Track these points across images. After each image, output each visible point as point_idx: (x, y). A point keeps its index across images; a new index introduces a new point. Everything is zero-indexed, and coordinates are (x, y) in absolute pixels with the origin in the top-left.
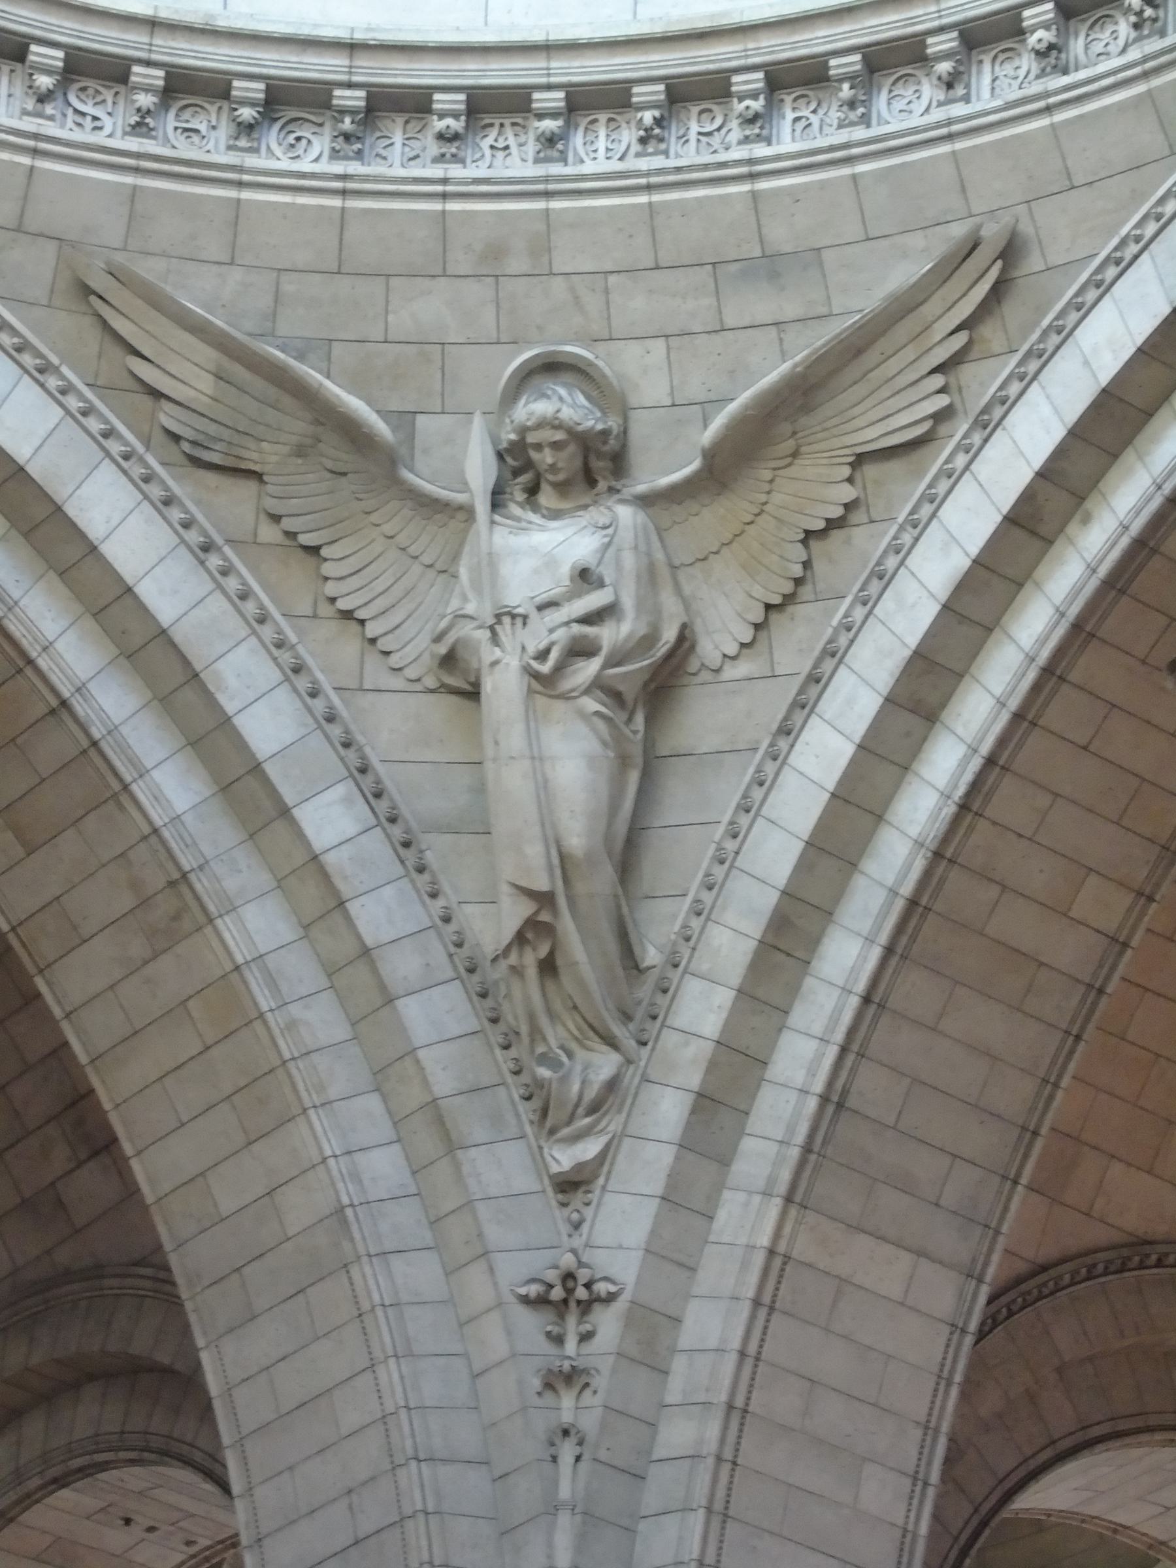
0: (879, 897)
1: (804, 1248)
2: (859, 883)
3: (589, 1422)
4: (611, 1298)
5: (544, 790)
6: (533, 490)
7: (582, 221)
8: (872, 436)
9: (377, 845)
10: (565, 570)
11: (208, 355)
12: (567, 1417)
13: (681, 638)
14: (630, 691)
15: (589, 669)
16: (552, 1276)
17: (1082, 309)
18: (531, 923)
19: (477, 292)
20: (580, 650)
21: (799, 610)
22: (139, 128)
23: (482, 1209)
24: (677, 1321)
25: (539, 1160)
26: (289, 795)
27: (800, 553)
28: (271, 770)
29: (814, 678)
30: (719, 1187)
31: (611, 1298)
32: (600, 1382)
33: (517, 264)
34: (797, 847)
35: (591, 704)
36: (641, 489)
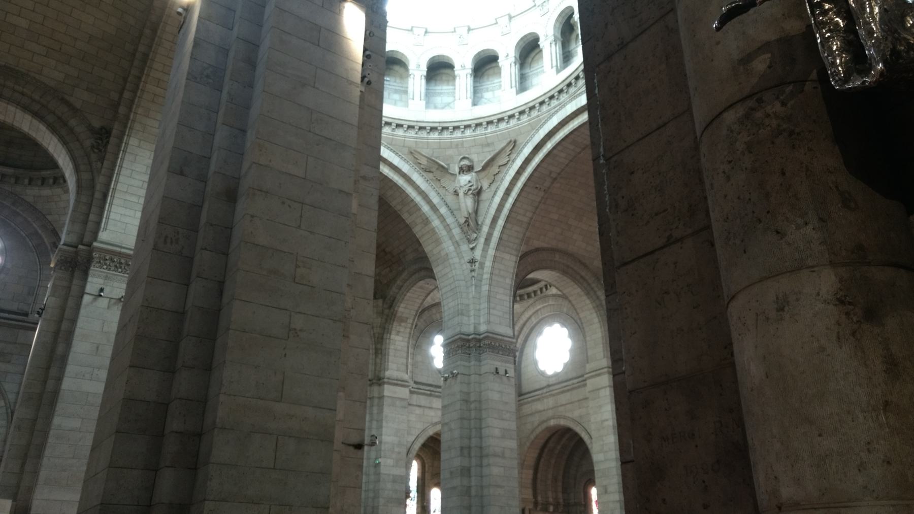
1: (498, 255)
2: (502, 214)
3: (476, 275)
5: (467, 206)
6: (463, 172)
7: (466, 141)
8: (501, 163)
9: (449, 213)
11: (426, 159)
14: (475, 194)
15: (471, 192)
17: (523, 148)
22: (416, 134)
24: (484, 263)
25: (468, 246)
28: (436, 206)
30: (488, 248)
31: (477, 261)
32: (477, 271)
35: (471, 196)
36: (475, 171)
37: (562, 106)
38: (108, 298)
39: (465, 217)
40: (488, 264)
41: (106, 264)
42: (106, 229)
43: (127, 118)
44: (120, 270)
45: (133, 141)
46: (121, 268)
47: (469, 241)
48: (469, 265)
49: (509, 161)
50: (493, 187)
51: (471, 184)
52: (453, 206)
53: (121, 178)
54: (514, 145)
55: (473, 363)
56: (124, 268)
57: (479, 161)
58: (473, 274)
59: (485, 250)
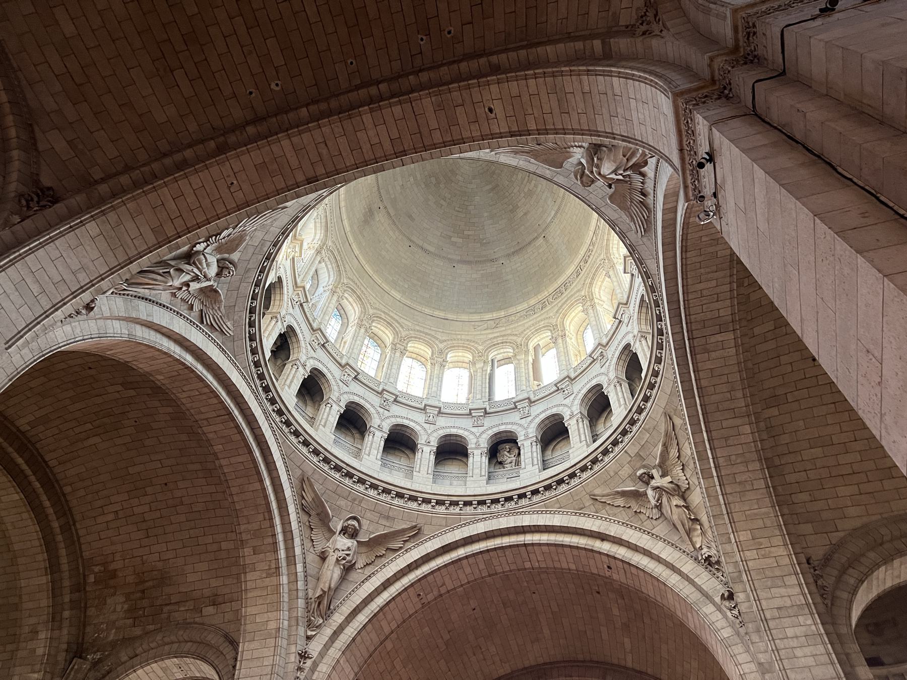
4: (311, 658)
6: (344, 534)
8: (390, 546)
10: (346, 547)
11: (313, 495)
12: (298, 675)
13: (355, 562)
14: (346, 567)
16: (304, 651)
18: (321, 595)
19: (350, 504)
20: (344, 559)
21: (371, 566)
27: (374, 558)
29: (370, 576)
31: (311, 658)
32: (306, 671)
35: (342, 567)
37: (497, 516)
39: (322, 590)
43: (102, 201)
45: (92, 228)
47: (310, 625)
49: (401, 548)
52: (312, 570)
54: (415, 533)
59: (327, 647)
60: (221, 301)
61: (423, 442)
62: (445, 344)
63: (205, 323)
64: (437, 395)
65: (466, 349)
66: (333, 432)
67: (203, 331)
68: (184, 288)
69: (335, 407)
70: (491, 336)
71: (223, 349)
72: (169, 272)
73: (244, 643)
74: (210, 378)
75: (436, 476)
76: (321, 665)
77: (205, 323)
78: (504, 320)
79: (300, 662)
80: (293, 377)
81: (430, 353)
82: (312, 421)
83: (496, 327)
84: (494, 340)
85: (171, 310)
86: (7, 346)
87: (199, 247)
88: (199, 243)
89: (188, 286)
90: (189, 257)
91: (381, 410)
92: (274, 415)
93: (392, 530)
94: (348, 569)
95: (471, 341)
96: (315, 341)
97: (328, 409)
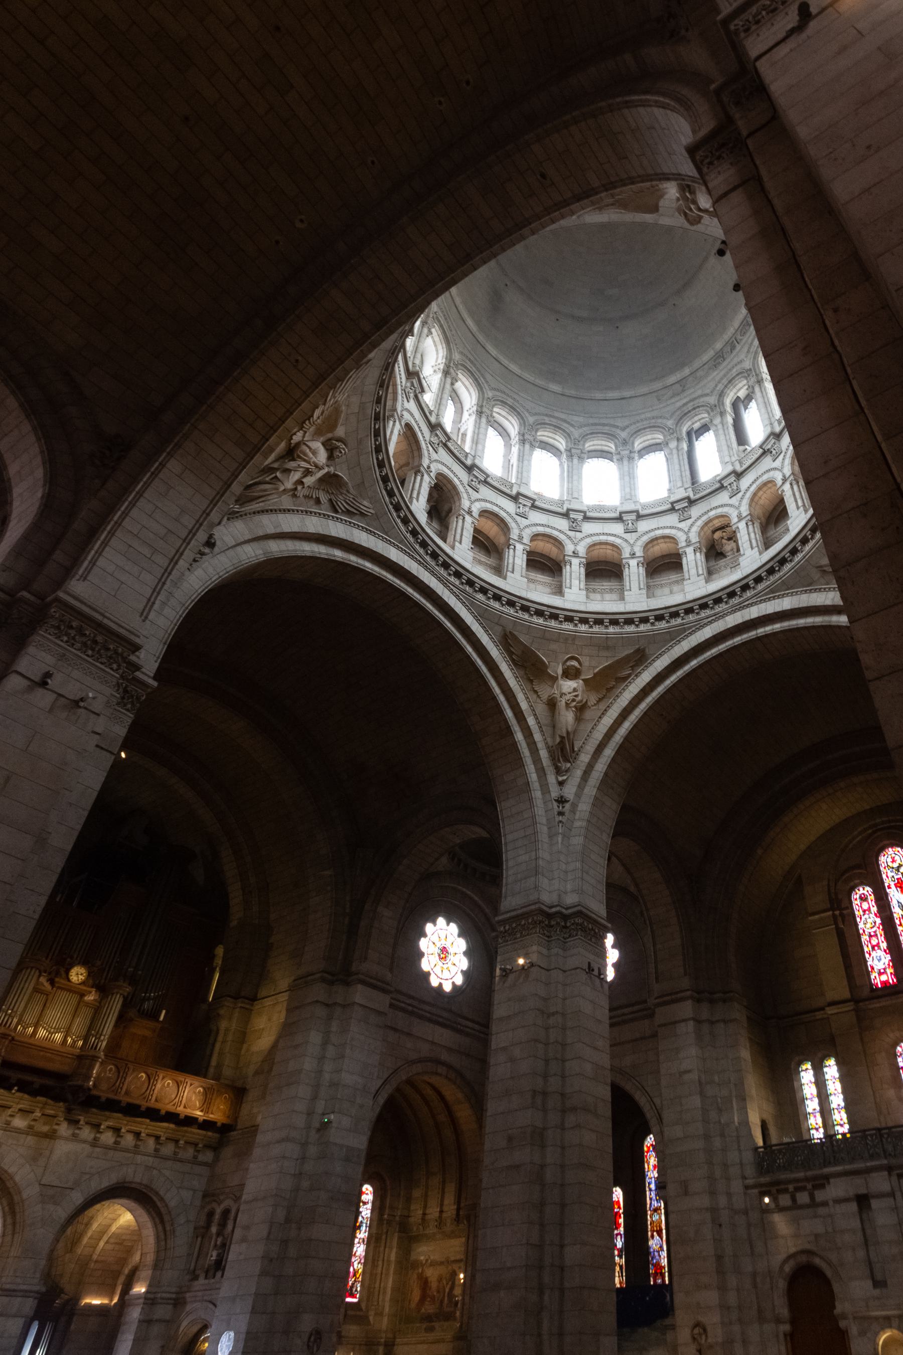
0: (614, 744)
3: (563, 820)
4: (568, 801)
8: (619, 675)
15: (574, 703)
22: (517, 612)
23: (550, 785)
24: (577, 806)
26: (526, 716)
29: (605, 710)
31: (568, 801)
33: (570, 642)
34: (603, 735)
38: (56, 693)
40: (584, 807)
41: (67, 634)
42: (85, 579)
44: (90, 652)
45: (174, 466)
46: (93, 650)
47: (558, 771)
48: (555, 804)
50: (602, 706)
51: (576, 693)
53: (134, 512)
55: (555, 951)
56: (99, 652)
57: (592, 665)
58: (561, 818)
59: (581, 787)
60: (347, 483)
61: (628, 556)
62: (628, 430)
63: (340, 511)
64: (631, 495)
65: (654, 427)
66: (524, 574)
67: (341, 520)
68: (299, 488)
69: (520, 547)
70: (679, 404)
71: (370, 531)
72: (276, 477)
73: (500, 803)
74: (368, 565)
75: (650, 590)
76: (580, 805)
77: (340, 511)
78: (691, 379)
79: (559, 807)
80: (462, 529)
81: (614, 447)
82: (499, 570)
83: (683, 391)
84: (685, 408)
85: (298, 511)
86: (143, 618)
87: (297, 438)
88: (295, 434)
89: (302, 483)
90: (292, 453)
91: (571, 534)
92: (452, 579)
93: (616, 659)
94: (581, 709)
95: (657, 418)
96: (474, 480)
97: (511, 551)
